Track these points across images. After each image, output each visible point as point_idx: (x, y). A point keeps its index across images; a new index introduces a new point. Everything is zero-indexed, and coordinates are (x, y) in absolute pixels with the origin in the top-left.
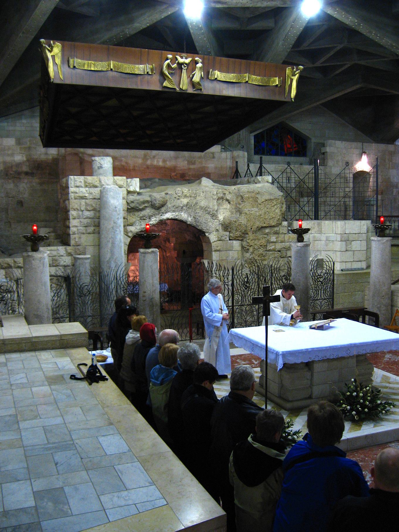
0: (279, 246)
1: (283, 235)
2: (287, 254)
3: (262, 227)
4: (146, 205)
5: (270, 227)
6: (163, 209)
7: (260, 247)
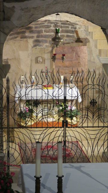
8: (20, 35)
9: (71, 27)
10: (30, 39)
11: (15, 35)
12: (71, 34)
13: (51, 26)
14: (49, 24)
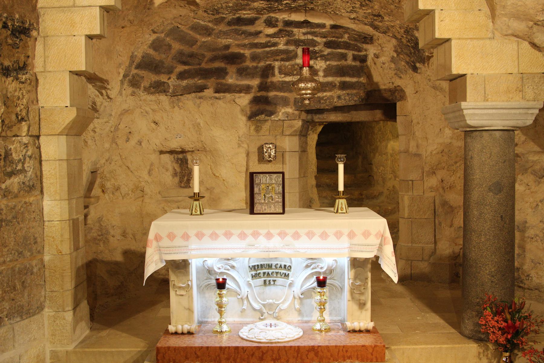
8: (211, 82)
9: (353, 55)
10: (242, 94)
11: (196, 80)
12: (354, 80)
13: (296, 56)
14: (292, 48)
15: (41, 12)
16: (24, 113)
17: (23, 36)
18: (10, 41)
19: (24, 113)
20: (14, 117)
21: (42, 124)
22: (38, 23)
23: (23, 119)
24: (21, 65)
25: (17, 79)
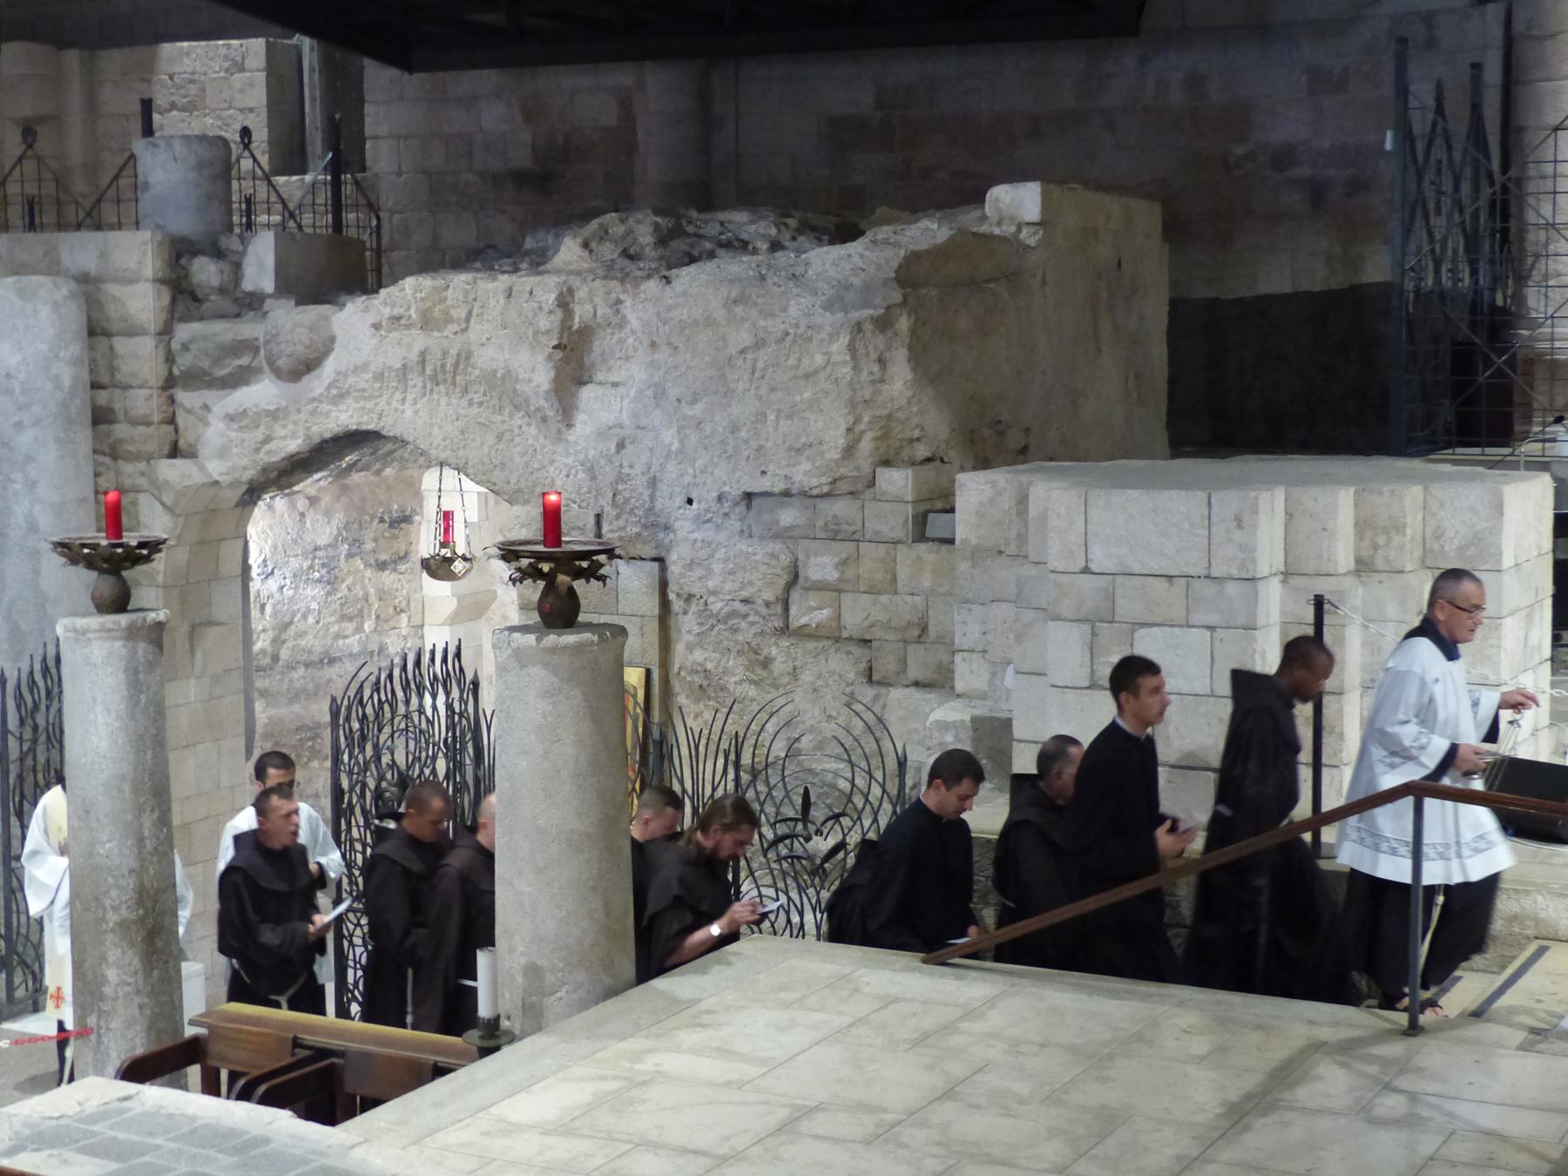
0: (856, 613)
1: (882, 549)
2: (903, 661)
3: (749, 497)
4: (245, 361)
5: (804, 494)
6: (317, 383)
7: (742, 608)
15: (425, 494)
16: (403, 605)
17: (402, 525)
18: (387, 534)
19: (403, 605)
20: (391, 610)
21: (426, 613)
22: (421, 507)
23: (402, 611)
24: (402, 554)
25: (395, 570)
